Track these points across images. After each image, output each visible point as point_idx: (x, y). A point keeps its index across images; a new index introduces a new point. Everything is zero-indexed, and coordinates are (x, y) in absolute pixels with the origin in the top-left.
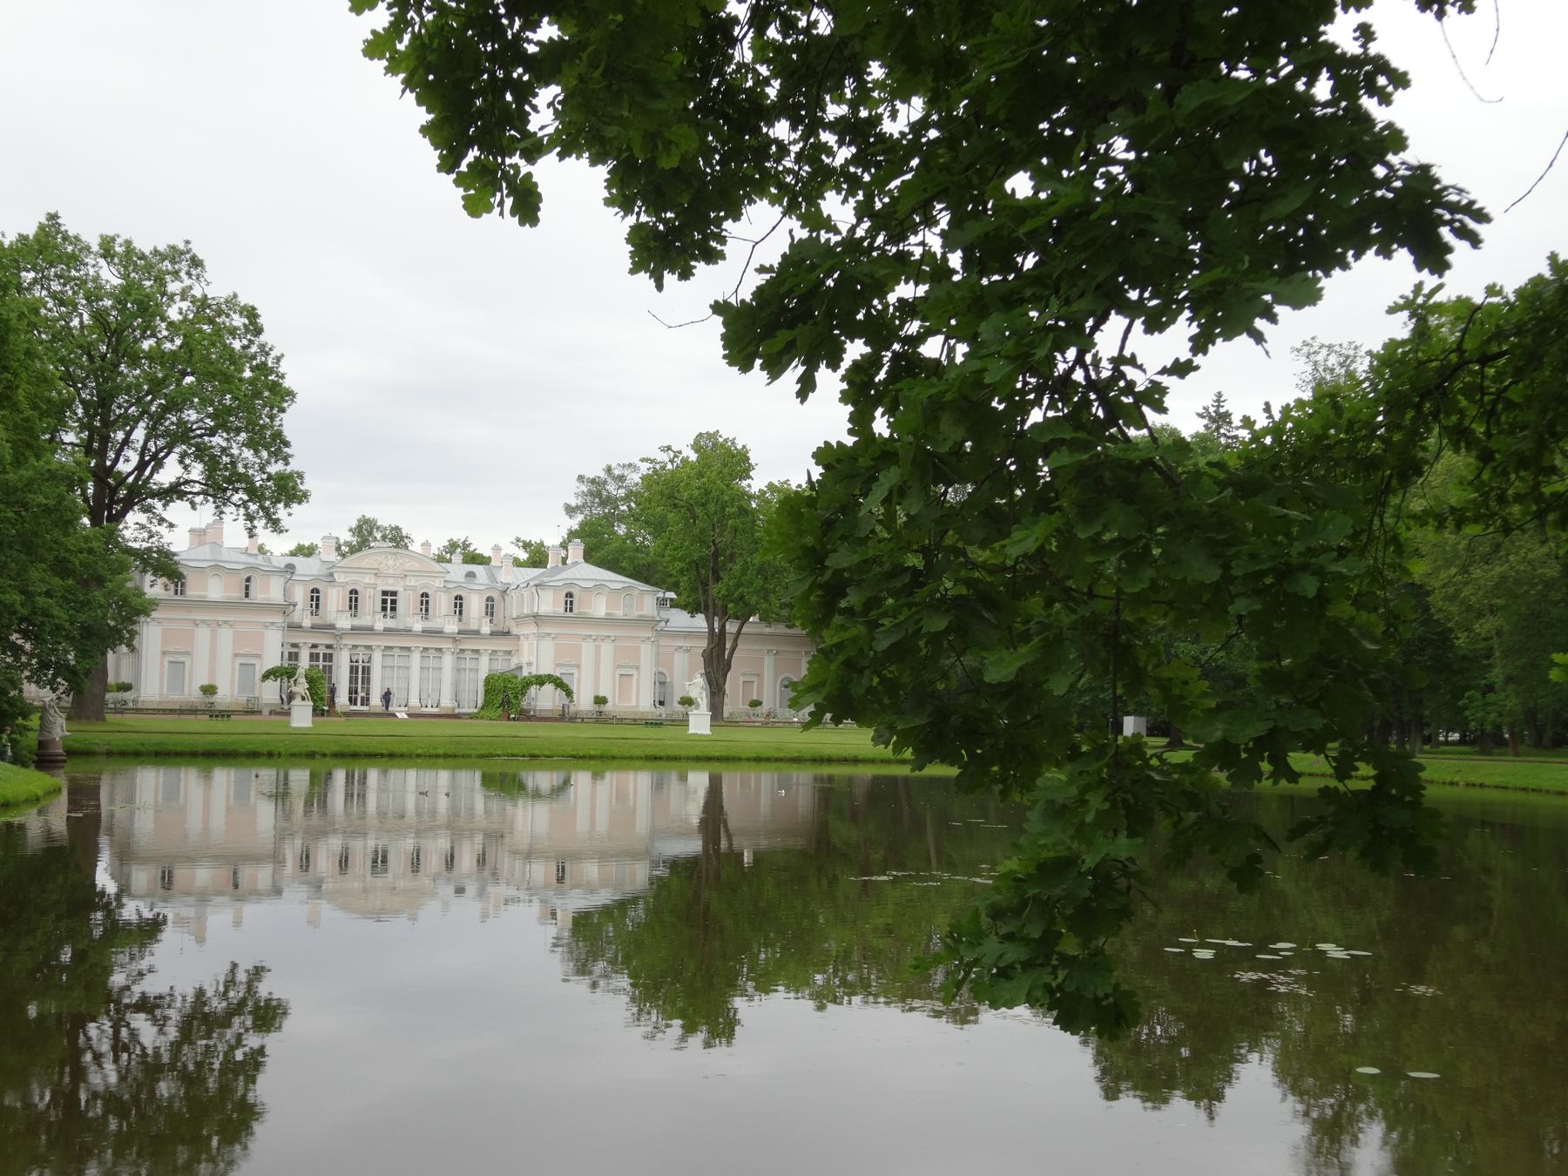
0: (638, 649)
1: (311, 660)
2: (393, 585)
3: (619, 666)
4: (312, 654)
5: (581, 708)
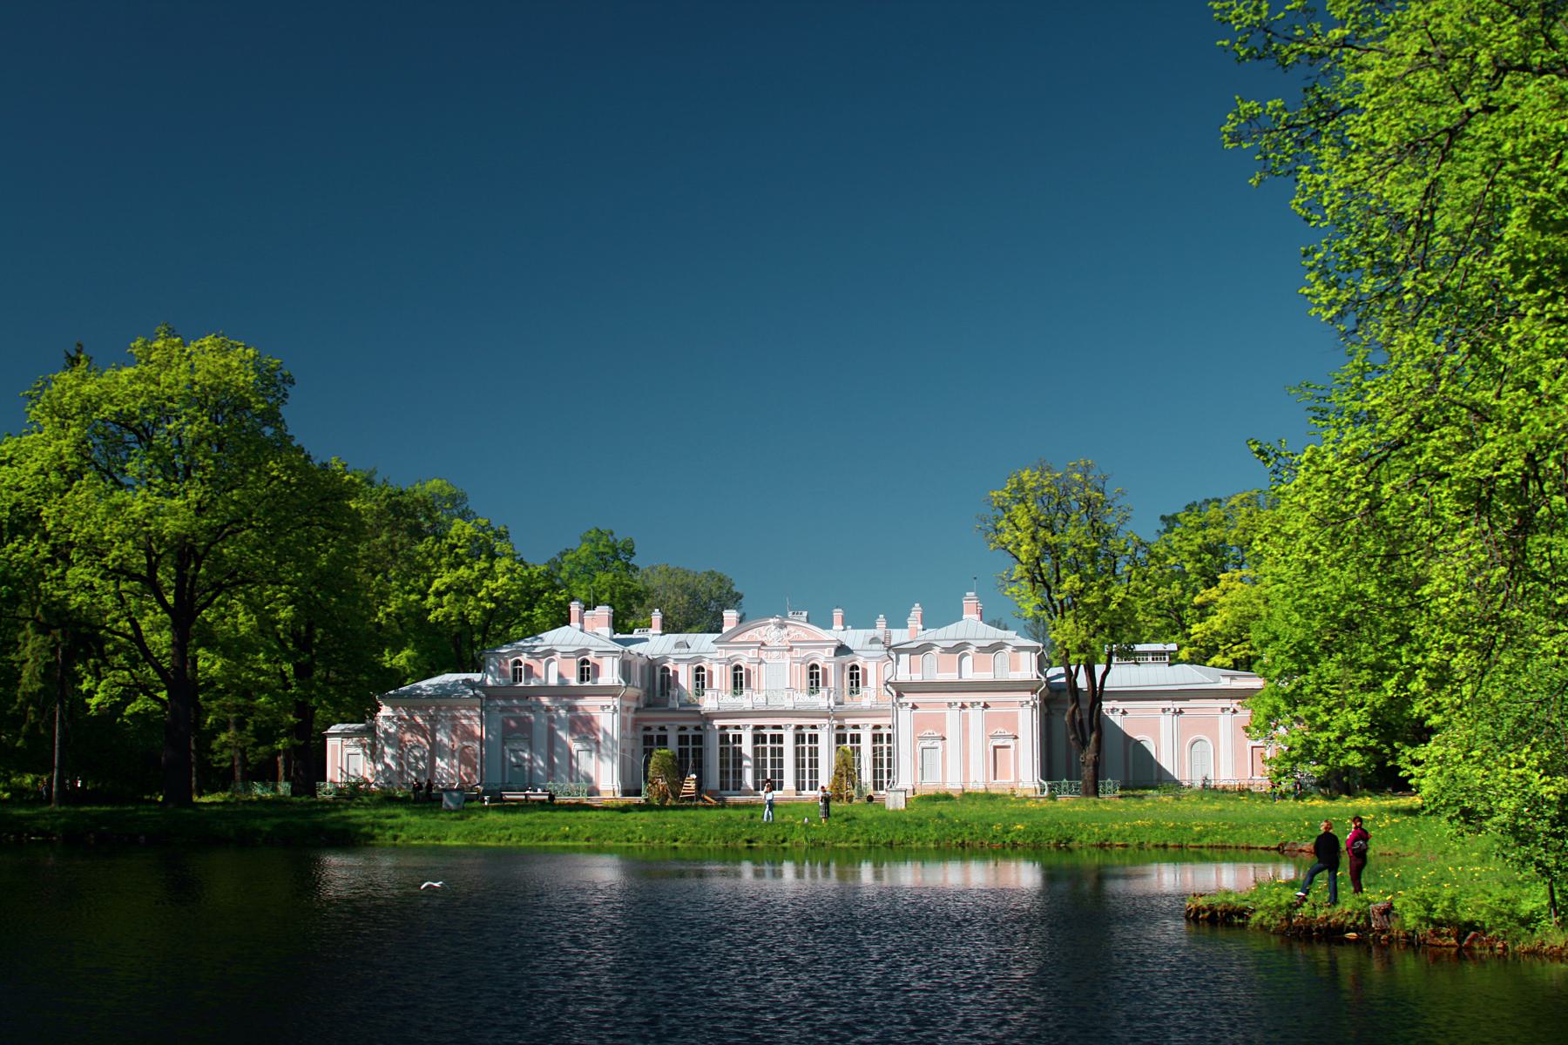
0: (1015, 715)
1: (680, 743)
2: (778, 658)
3: (992, 737)
4: (680, 737)
5: (948, 786)
